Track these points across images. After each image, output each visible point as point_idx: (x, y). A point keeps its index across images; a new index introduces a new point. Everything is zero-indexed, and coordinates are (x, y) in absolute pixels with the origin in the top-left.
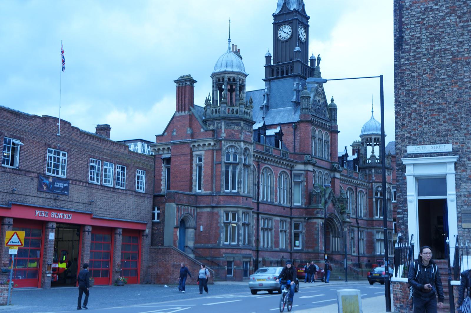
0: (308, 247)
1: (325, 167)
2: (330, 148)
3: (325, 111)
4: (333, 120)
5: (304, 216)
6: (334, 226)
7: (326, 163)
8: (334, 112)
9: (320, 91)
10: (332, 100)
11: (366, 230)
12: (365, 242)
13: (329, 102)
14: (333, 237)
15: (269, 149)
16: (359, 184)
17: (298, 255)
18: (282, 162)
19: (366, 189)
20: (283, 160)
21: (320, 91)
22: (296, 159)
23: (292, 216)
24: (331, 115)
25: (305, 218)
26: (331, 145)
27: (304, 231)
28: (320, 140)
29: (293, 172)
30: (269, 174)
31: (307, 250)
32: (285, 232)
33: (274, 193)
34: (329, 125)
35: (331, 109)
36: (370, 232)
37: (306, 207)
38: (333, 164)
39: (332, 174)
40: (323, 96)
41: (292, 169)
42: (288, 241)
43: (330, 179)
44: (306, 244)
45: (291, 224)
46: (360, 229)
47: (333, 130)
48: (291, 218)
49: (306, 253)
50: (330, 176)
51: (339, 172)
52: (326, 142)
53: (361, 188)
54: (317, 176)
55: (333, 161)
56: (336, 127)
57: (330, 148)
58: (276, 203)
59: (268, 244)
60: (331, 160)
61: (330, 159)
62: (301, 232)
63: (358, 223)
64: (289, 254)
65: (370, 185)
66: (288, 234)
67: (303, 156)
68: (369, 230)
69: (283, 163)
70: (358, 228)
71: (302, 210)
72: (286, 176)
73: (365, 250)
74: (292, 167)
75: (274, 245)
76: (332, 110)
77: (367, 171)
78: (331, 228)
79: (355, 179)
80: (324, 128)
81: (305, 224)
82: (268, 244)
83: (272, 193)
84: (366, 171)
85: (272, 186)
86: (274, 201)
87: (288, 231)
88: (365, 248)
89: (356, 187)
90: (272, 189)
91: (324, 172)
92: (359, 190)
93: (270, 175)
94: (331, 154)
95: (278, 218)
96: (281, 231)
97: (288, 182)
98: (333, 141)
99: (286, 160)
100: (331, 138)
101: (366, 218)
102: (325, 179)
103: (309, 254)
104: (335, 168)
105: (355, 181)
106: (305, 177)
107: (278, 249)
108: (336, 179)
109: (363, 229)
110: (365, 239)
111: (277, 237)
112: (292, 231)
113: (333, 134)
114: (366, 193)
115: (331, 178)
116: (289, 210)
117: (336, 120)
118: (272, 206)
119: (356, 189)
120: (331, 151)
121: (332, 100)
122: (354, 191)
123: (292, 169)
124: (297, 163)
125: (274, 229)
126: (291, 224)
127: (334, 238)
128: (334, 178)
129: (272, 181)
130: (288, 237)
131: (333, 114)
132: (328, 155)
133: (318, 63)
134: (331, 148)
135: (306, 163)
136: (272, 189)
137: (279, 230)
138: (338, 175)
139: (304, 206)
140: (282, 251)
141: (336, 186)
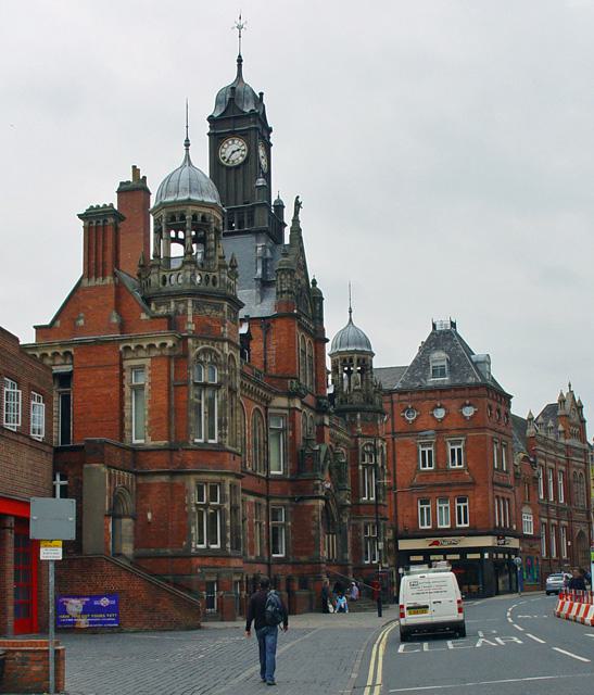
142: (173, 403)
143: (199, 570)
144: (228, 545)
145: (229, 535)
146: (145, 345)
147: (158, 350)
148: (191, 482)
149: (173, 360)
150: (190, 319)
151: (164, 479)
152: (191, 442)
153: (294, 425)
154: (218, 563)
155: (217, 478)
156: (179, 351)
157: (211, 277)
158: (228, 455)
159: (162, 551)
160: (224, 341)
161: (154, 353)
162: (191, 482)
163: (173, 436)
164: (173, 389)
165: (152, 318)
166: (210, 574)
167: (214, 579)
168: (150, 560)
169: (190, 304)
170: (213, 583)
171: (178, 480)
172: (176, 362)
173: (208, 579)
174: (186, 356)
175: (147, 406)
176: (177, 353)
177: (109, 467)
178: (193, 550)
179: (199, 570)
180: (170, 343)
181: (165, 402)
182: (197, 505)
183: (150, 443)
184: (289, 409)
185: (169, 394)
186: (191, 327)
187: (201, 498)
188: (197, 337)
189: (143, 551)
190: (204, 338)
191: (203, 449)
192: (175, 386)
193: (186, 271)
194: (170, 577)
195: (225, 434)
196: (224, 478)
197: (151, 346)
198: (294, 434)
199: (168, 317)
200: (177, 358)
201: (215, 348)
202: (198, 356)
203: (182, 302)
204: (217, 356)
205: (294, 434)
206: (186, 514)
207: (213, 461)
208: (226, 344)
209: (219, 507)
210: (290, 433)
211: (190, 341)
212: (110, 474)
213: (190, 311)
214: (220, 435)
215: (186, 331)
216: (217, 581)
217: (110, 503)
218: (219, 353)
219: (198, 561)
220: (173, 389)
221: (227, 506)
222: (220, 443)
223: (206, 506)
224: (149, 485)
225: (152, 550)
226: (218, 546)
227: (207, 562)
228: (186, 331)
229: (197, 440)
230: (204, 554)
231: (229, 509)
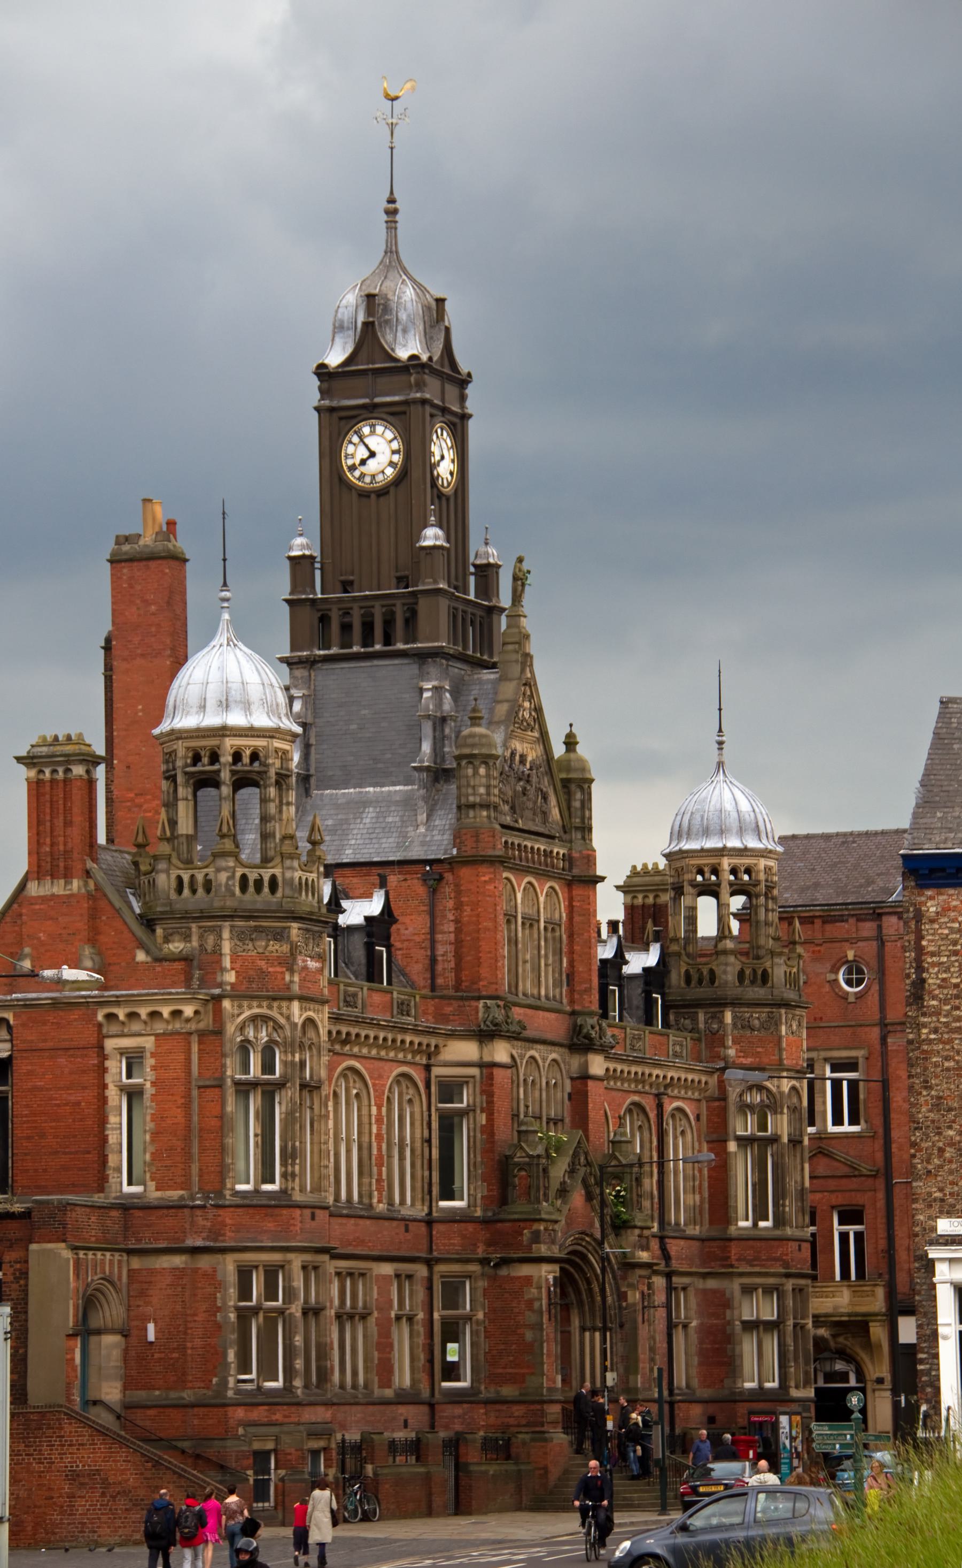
0: (496, 1380)
1: (549, 1036)
2: (565, 950)
3: (545, 798)
4: (577, 828)
5: (481, 1252)
6: (589, 1283)
7: (553, 1016)
8: (579, 796)
9: (527, 715)
10: (570, 743)
11: (700, 1284)
12: (694, 1337)
13: (559, 750)
14: (583, 1329)
15: (355, 995)
16: (672, 1084)
17: (458, 1410)
18: (399, 1038)
19: (699, 1100)
20: (404, 1030)
21: (527, 715)
22: (444, 1019)
23: (435, 1254)
24: (567, 809)
25: (484, 1262)
26: (571, 936)
27: (480, 1315)
28: (531, 922)
29: (436, 1071)
30: (355, 1091)
31: (492, 1389)
32: (410, 1319)
33: (375, 1169)
34: (562, 852)
35: (566, 783)
36: (714, 1292)
37: (490, 1214)
38: (579, 1021)
39: (575, 1062)
40: (536, 734)
41: (432, 1061)
42: (422, 1357)
43: (568, 1083)
44: (489, 1365)
45: (430, 1288)
46: (675, 1279)
47: (576, 871)
48: (430, 1263)
49: (487, 1402)
50: (568, 1071)
51: (604, 1050)
52: (552, 925)
53: (677, 1098)
54: (522, 1078)
55: (577, 1008)
56: (590, 859)
57: (565, 950)
58: (381, 1207)
59: (355, 1373)
60: (572, 1002)
61: (565, 1001)
62: (469, 1318)
63: (666, 1256)
64: (425, 1409)
65: (713, 1080)
66: (422, 1330)
67: (474, 1003)
68: (712, 1284)
69: (403, 1042)
70: (669, 1276)
71: (470, 1227)
72: (411, 1091)
73: (694, 1372)
74: (432, 1053)
75: (376, 1379)
76: (573, 787)
77: (701, 1017)
78: (578, 1292)
79: (657, 1065)
80: (541, 869)
81: (482, 1284)
82: (355, 1373)
83: (366, 1169)
84: (695, 1020)
85: (366, 1139)
86: (375, 1200)
87: (421, 1316)
88: (695, 1360)
89: (658, 1096)
90: (365, 1152)
91: (544, 1060)
92: (670, 1106)
93: (357, 1095)
94: (570, 977)
95: (387, 1269)
96: (398, 1318)
97: (417, 1116)
98: (577, 919)
99: (416, 1031)
100: (571, 909)
101: (695, 1230)
102: (547, 1083)
103: (504, 1407)
104: (588, 1037)
105: (656, 1072)
106: (483, 1092)
107: (389, 1393)
108: (590, 1083)
109: (686, 1280)
110: (694, 1324)
111: (385, 1345)
112: (436, 1316)
113: (578, 891)
114: (698, 1118)
115: (572, 1079)
116: (423, 1229)
117: (590, 829)
118: (368, 1222)
119: (660, 1107)
120: (571, 963)
121: (570, 743)
122: (652, 1115)
123: (432, 1061)
124: (452, 1035)
125: (376, 1314)
126: (430, 1288)
127: (587, 1334)
128: (584, 1077)
129: (365, 1120)
130: (421, 1340)
131: (577, 804)
132: (557, 984)
133: (517, 598)
134: (571, 952)
135: (485, 1035)
136: (365, 1152)
137: (393, 1315)
138: (597, 1065)
139: (479, 1213)
140: (404, 1398)
141: (592, 1114)
142: (195, 1118)
143: (241, 1431)
144: (298, 1383)
145: (299, 1364)
146: (143, 1012)
147: (168, 1022)
148: (229, 1266)
149: (195, 1039)
150: (227, 962)
151: (178, 1261)
152: (227, 1193)
153: (490, 1102)
154: (278, 1417)
155: (276, 1257)
156: (207, 1022)
157: (266, 879)
158: (298, 1212)
159: (173, 1395)
160: (290, 999)
161: (159, 1027)
162: (229, 1266)
163: (195, 1179)
164: (195, 1093)
165: (158, 960)
166: (263, 1438)
167: (270, 1446)
168: (151, 1412)
169: (226, 934)
170: (267, 1453)
171: (204, 1262)
172: (200, 1043)
173: (257, 1446)
174: (218, 1032)
175: (150, 1126)
176: (202, 1026)
177: (75, 1249)
178: (230, 1393)
179: (241, 1431)
180: (188, 1011)
181: (181, 1119)
182: (238, 1309)
183: (154, 1195)
184: (481, 1065)
185: (187, 1106)
186: (231, 977)
187: (245, 1292)
188: (238, 995)
189: (140, 1395)
190: (253, 998)
191: (256, 1204)
192: (199, 1087)
193: (218, 870)
194: (185, 1445)
195: (293, 1175)
196: (290, 1256)
197: (155, 1015)
198: (490, 1119)
199: (186, 959)
200: (202, 1034)
201: (274, 1013)
202: (242, 1028)
203: (212, 929)
204: (278, 1027)
205: (490, 1119)
206: (219, 1327)
207: (270, 1225)
208: (296, 1005)
209: (281, 1312)
210: (483, 1119)
211: (226, 1004)
212: (77, 1262)
213: (226, 947)
214: (284, 1175)
215: (220, 985)
216: (275, 1450)
217: (76, 1315)
218: (282, 1021)
219: (240, 1413)
220: (195, 1093)
221: (296, 1310)
222: (284, 1191)
223: (255, 1310)
224: (152, 1272)
225: (157, 1393)
226: (278, 1384)
227: (258, 1414)
228: (220, 985)
229: (241, 1187)
230: (257, 1399)
231: (299, 1314)
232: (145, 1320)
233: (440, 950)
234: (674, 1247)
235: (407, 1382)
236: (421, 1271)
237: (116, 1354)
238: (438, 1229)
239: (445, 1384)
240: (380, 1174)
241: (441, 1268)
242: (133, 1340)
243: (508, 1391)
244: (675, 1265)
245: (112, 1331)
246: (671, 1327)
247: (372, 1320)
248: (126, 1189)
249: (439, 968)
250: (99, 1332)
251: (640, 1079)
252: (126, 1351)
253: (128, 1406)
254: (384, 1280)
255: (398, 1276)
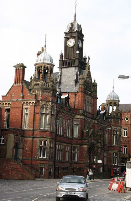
3: (91, 87)
10: (95, 81)
13: (93, 82)
14: (92, 155)
17: (75, 164)
24: (94, 89)
26: (94, 105)
32: (69, 152)
56: (96, 95)
59: (60, 158)
80: (90, 95)
82: (60, 158)
95: (65, 144)
100: (94, 101)
116: (71, 140)
121: (95, 81)
140: (67, 162)
167: (43, 167)
168: (26, 161)
170: (43, 168)
173: (41, 166)
219: (39, 161)
227: (42, 162)
232: (26, 147)
233: (76, 104)
234: (105, 147)
235: (68, 160)
236: (70, 145)
237: (22, 152)
238: (73, 140)
239: (73, 161)
240: (65, 131)
241: (73, 145)
242: (24, 150)
243: (82, 162)
244: (105, 149)
245: (22, 149)
246: (104, 157)
247: (63, 151)
248: (25, 128)
249: (76, 106)
250: (19, 148)
251: (102, 126)
252: (23, 152)
253: (23, 159)
254: (65, 146)
255: (67, 146)
